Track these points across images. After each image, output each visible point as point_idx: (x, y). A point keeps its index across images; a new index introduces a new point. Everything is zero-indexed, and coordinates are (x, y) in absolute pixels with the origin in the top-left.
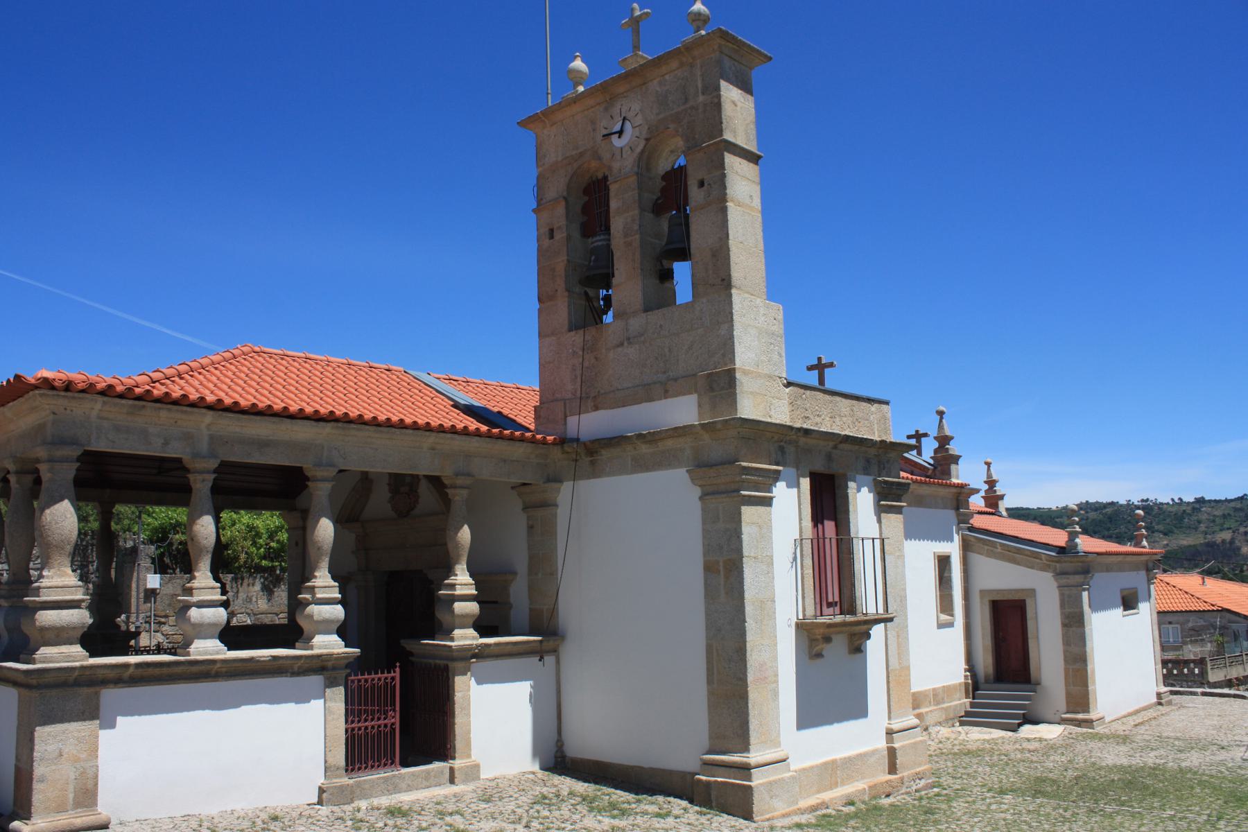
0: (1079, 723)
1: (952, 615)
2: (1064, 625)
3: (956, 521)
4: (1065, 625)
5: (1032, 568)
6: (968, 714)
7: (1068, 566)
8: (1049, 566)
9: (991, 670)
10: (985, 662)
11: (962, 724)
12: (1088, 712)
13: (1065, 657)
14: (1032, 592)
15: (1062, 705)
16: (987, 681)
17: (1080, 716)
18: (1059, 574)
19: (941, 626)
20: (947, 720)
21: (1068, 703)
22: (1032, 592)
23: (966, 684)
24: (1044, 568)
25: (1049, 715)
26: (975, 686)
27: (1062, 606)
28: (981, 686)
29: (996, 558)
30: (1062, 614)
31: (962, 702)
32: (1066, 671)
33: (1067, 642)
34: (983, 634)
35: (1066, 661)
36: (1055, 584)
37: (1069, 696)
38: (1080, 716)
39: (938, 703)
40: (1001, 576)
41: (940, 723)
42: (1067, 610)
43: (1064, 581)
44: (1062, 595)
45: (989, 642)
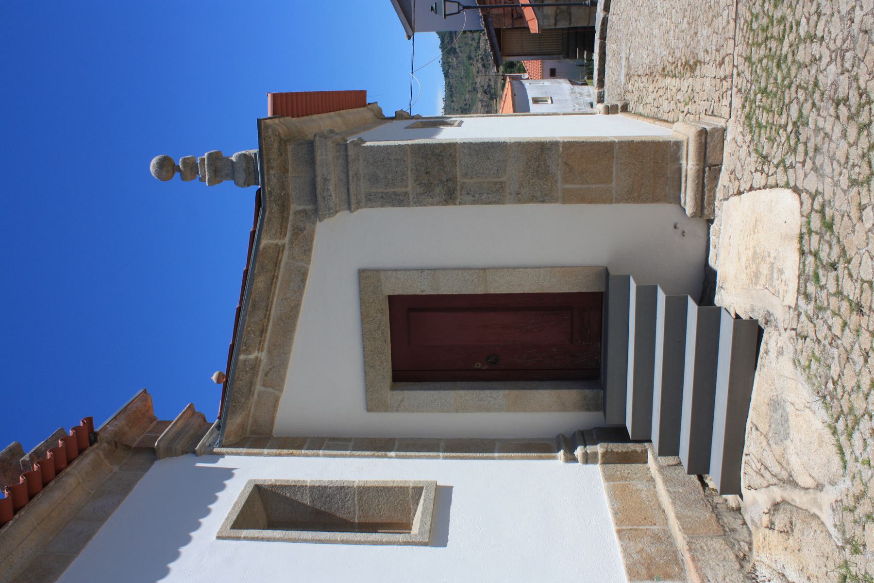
0: (709, 169)
1: (418, 491)
2: (450, 197)
3: (188, 458)
4: (450, 196)
5: (303, 275)
6: (699, 466)
7: (295, 183)
8: (298, 231)
9: (571, 395)
10: (548, 408)
11: (731, 483)
12: (678, 144)
13: (533, 199)
14: (367, 278)
15: (663, 212)
16: (600, 405)
17: (689, 165)
18: (316, 207)
19: (438, 536)
20: (726, 533)
21: (655, 199)
22: (367, 278)
23: (609, 459)
24: (304, 242)
25: (691, 248)
26: (609, 435)
27: (399, 200)
28: (613, 420)
29: (284, 364)
30: (419, 203)
31: (657, 476)
32: (570, 198)
33: (494, 194)
34: (479, 409)
35: (544, 198)
36: (343, 216)
37: (636, 194)
38: (689, 165)
39: (675, 559)
40: (328, 356)
41: (742, 559)
42: (410, 187)
43: (333, 190)
44: (372, 200)
45: (500, 395)
